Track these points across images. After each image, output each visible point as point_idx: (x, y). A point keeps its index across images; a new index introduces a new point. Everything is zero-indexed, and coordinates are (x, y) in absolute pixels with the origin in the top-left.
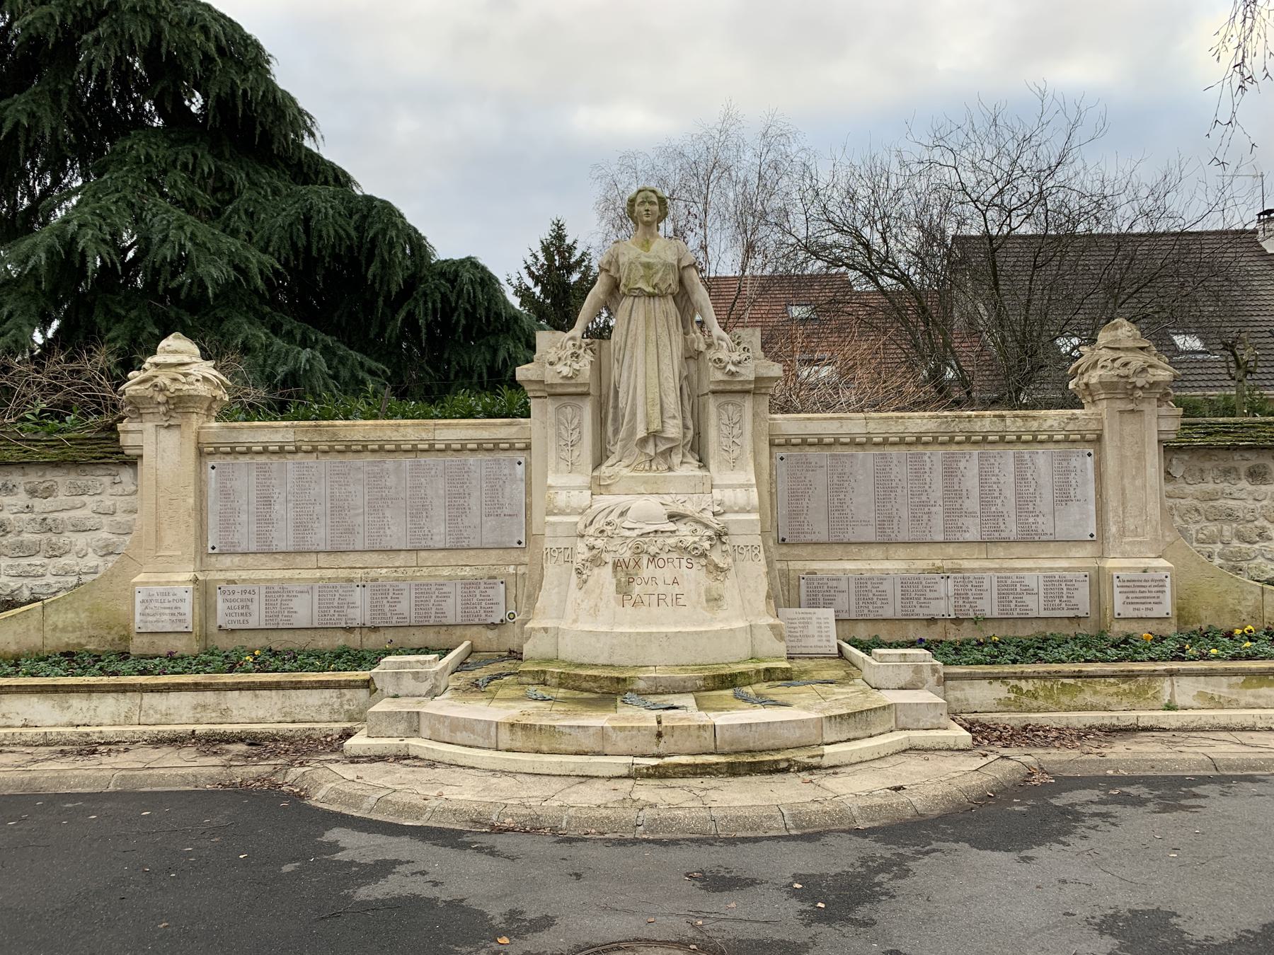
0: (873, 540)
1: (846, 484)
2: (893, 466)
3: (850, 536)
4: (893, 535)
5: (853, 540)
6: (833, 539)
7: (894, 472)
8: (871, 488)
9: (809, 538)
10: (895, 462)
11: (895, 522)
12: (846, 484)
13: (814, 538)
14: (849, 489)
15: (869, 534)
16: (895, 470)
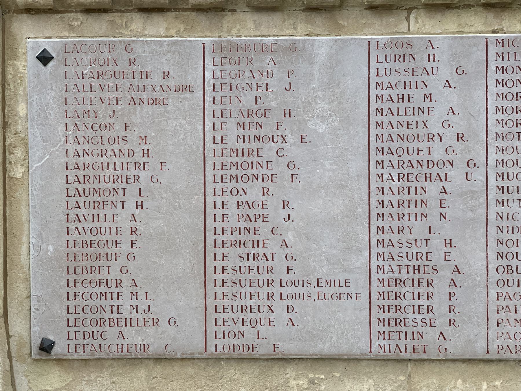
0: (359, 345)
1: (268, 151)
2: (436, 84)
3: (279, 334)
4: (431, 335)
5: (287, 347)
6: (218, 345)
7: (440, 110)
8: (357, 165)
9: (135, 338)
10: (445, 72)
11: (441, 287)
12: (268, 151)
13: (154, 339)
14: (279, 168)
15: (346, 326)
16: (445, 99)
